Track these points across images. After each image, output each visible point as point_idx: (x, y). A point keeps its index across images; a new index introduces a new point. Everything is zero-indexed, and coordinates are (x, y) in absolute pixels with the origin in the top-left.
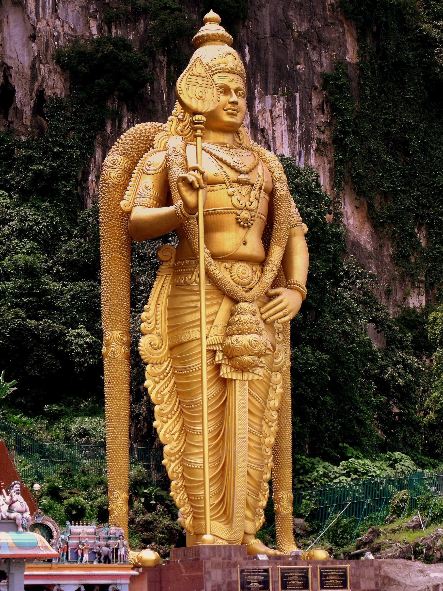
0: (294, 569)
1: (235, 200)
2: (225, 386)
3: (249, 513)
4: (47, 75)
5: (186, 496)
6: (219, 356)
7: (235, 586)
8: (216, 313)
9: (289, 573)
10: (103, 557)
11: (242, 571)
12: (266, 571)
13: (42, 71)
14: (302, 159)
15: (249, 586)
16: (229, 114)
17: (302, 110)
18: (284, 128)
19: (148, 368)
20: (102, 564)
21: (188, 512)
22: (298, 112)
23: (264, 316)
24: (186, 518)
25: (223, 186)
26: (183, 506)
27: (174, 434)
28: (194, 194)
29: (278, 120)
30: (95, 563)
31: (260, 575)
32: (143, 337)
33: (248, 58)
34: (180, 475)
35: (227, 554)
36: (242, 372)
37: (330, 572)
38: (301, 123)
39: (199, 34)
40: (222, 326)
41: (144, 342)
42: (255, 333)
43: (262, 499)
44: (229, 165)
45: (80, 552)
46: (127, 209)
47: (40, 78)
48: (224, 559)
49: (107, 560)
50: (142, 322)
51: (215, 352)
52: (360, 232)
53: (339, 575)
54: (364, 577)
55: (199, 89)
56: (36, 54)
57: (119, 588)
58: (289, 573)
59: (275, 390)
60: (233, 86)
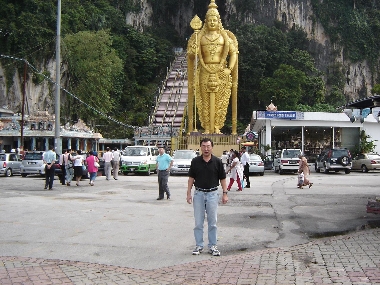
3: (218, 125)
14: (304, 21)
18: (298, 13)
20: (170, 136)
22: (302, 8)
23: (219, 76)
25: (207, 45)
28: (195, 49)
29: (296, 11)
30: (168, 135)
38: (304, 11)
39: (209, 6)
44: (209, 40)
47: (232, 8)
49: (171, 135)
52: (322, 41)
60: (212, 19)
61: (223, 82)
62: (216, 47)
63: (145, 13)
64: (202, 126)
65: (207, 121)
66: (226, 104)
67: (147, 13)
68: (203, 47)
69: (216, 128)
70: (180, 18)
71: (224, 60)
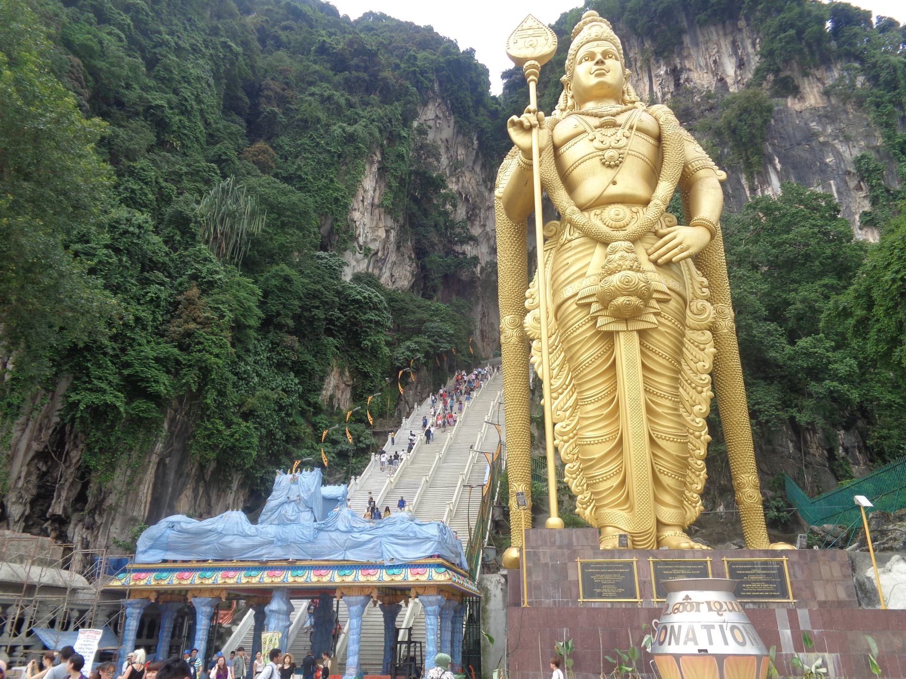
0: (679, 563)
1: (596, 143)
3: (667, 498)
5: (584, 481)
6: (595, 307)
7: (574, 590)
8: (588, 264)
9: (671, 569)
11: (585, 566)
12: (629, 565)
15: (598, 591)
16: (598, 75)
17: (838, 192)
19: (534, 344)
21: (588, 501)
23: (652, 257)
24: (586, 509)
26: (582, 493)
27: (565, 411)
31: (617, 573)
32: (528, 315)
33: (779, 166)
35: (566, 541)
36: (626, 320)
37: (750, 569)
40: (595, 275)
41: (528, 320)
42: (629, 269)
43: (696, 481)
46: (500, 195)
48: (560, 547)
50: (526, 299)
51: (589, 305)
53: (768, 575)
54: (821, 579)
55: (528, 39)
58: (671, 569)
59: (703, 350)
61: (676, 286)
62: (627, 133)
63: (392, 276)
64: (586, 512)
65: (603, 486)
66: (699, 396)
67: (397, 275)
68: (562, 150)
69: (665, 519)
70: (481, 319)
71: (665, 188)
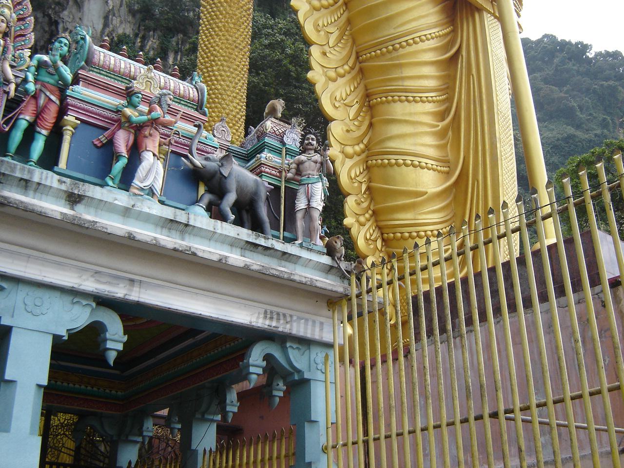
2: (454, 31)
4: (118, 25)
10: (231, 198)
13: (114, 22)
34: (364, 187)
45: (122, 141)
47: (111, 26)
56: (111, 8)
57: (298, 359)
